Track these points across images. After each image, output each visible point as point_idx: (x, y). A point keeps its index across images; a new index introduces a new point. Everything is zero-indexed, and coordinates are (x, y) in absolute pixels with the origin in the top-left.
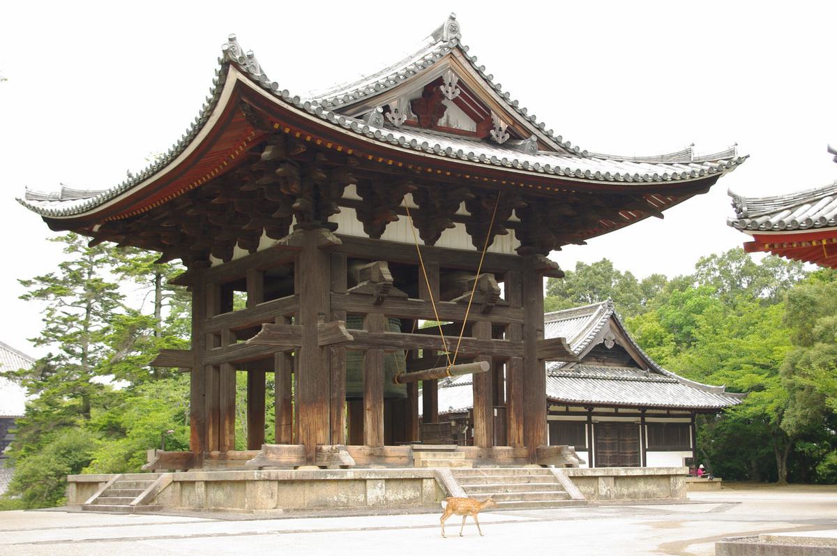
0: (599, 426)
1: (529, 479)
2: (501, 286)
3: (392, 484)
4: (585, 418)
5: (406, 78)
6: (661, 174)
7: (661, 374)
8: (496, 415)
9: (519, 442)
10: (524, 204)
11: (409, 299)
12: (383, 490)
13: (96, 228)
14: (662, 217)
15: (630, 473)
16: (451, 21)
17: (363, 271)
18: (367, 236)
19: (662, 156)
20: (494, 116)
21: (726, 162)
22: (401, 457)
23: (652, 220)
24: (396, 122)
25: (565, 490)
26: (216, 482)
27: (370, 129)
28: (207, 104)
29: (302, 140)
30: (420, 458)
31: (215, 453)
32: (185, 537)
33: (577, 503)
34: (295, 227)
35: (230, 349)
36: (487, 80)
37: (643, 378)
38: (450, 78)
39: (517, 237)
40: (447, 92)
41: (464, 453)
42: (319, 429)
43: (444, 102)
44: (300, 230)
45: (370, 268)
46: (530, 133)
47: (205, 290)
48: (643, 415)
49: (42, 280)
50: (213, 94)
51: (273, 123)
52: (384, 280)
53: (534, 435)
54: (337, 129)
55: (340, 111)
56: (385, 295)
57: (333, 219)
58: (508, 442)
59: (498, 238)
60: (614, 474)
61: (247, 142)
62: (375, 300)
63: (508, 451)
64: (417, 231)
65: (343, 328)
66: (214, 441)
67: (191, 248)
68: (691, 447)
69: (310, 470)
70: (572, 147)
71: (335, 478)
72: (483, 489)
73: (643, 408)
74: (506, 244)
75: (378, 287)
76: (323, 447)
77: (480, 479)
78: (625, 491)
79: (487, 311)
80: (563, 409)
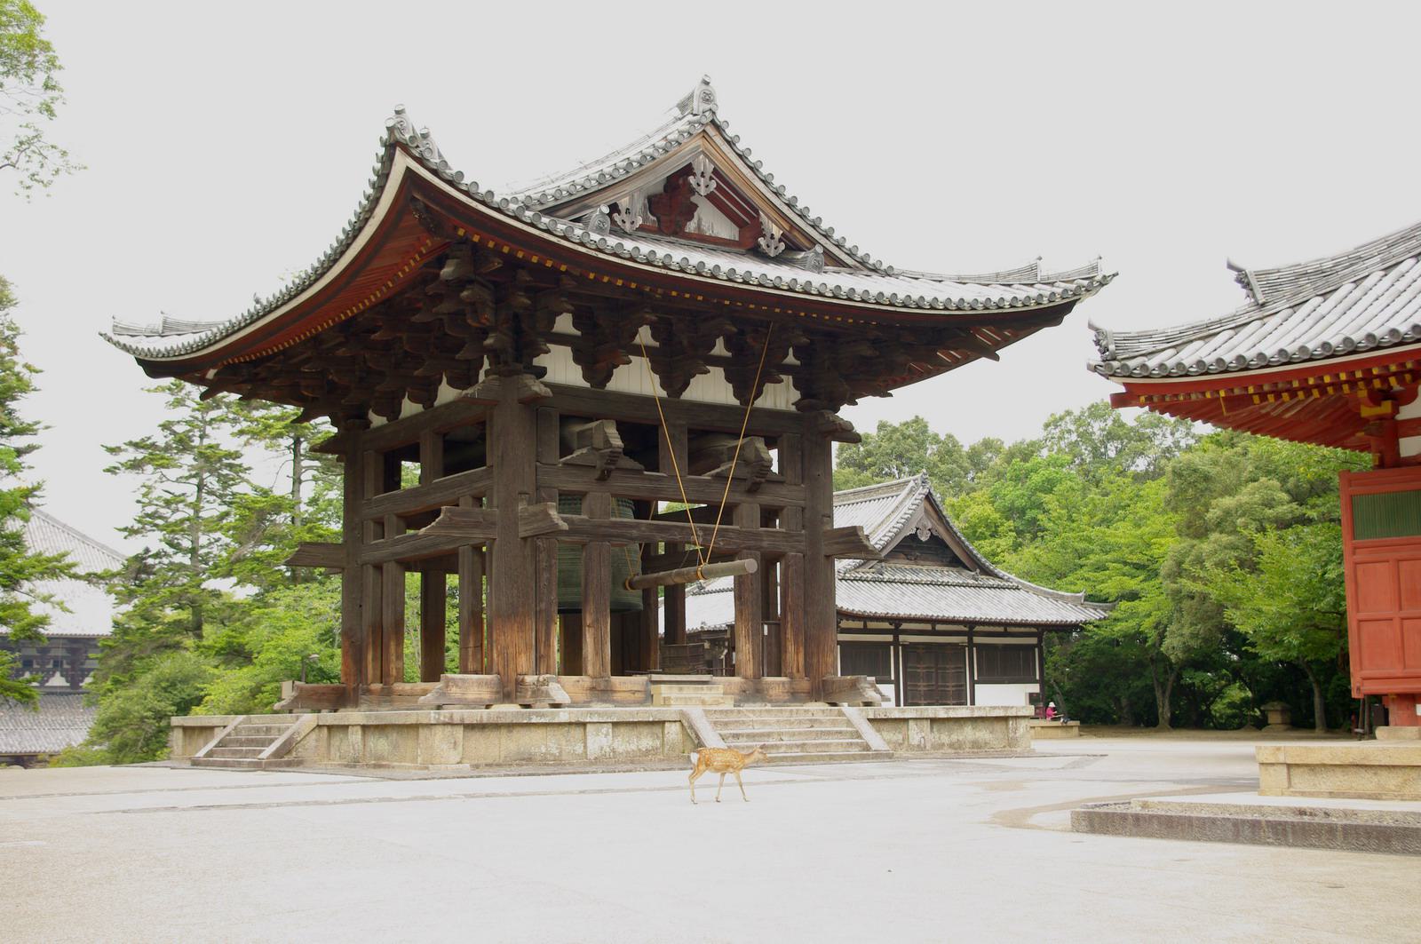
0: (910, 649)
1: (813, 722)
2: (774, 454)
3: (622, 730)
4: (890, 638)
5: (641, 165)
6: (995, 299)
7: (996, 576)
8: (766, 633)
9: (798, 671)
10: (804, 340)
11: (646, 473)
12: (610, 737)
13: (211, 374)
14: (997, 358)
15: (952, 714)
16: (704, 87)
17: (581, 434)
18: (587, 385)
19: (997, 275)
20: (763, 218)
21: (1086, 283)
22: (634, 692)
23: (983, 363)
24: (627, 227)
25: (862, 739)
26: (377, 727)
27: (589, 236)
28: (365, 202)
29: (497, 252)
30: (661, 694)
31: (377, 686)
32: (335, 803)
33: (878, 756)
34: (487, 373)
35: (397, 542)
36: (753, 169)
37: (971, 582)
38: (703, 165)
39: (796, 386)
40: (699, 185)
41: (721, 686)
42: (520, 654)
43: (694, 199)
44: (495, 376)
45: (591, 429)
46: (814, 242)
47: (363, 460)
48: (970, 634)
49: (136, 445)
50: (374, 188)
51: (456, 228)
52: (611, 446)
53: (819, 662)
54: (546, 236)
55: (550, 212)
56: (613, 467)
57: (539, 361)
58: (783, 670)
59: (769, 387)
60: (931, 716)
61: (421, 254)
62: (597, 474)
63: (783, 683)
64: (657, 378)
65: (554, 513)
66: (374, 669)
67: (343, 401)
68: (1038, 678)
69: (509, 710)
70: (871, 262)
71: (543, 720)
72: (748, 736)
73: (897, 621)
74: (780, 396)
75: (602, 456)
76: (526, 677)
77: (744, 722)
78: (945, 738)
79: (753, 490)
80: (860, 625)
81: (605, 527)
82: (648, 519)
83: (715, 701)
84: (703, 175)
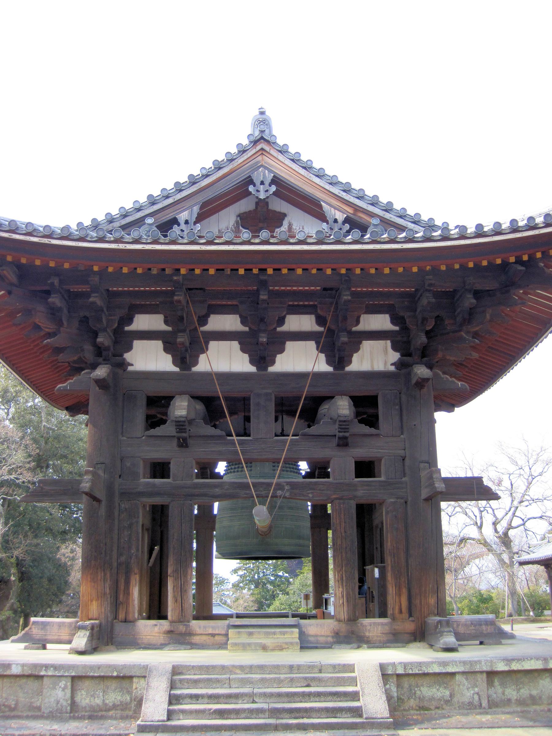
9: (401, 612)
18: (177, 369)
22: (213, 635)
39: (395, 348)
40: (258, 191)
42: (92, 601)
53: (421, 602)
56: (184, 435)
63: (382, 624)
64: (246, 357)
77: (218, 681)
81: (186, 488)
83: (277, 646)
84: (262, 183)
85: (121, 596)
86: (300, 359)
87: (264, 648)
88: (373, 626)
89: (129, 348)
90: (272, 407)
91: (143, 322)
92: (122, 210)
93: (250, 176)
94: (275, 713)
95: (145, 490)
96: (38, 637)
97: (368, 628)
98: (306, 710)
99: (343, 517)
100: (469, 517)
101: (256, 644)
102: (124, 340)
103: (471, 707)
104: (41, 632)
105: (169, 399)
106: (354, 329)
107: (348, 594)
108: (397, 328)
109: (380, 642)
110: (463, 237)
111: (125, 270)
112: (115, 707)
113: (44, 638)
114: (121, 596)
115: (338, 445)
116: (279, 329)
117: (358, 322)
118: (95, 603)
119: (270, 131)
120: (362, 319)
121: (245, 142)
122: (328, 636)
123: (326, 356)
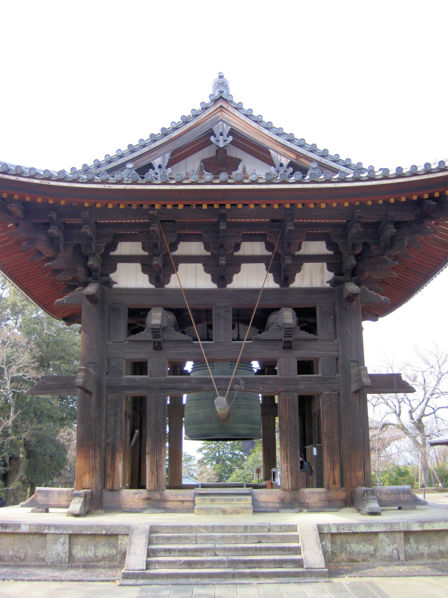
9: (334, 483)
18: (153, 287)
22: (183, 501)
40: (218, 141)
42: (85, 474)
53: (351, 474)
54: (6, 177)
56: (159, 340)
63: (320, 493)
64: (209, 276)
77: (187, 538)
82: (264, 375)
84: (221, 134)
85: (109, 471)
86: (253, 278)
87: (224, 512)
88: (312, 494)
89: (114, 269)
90: (230, 317)
91: (125, 248)
92: (108, 157)
93: (211, 129)
94: (233, 564)
95: (127, 384)
96: (42, 503)
97: (308, 496)
98: (258, 562)
99: (288, 406)
100: (390, 407)
101: (218, 509)
102: (110, 263)
103: (391, 560)
104: (46, 499)
105: (147, 310)
106: (297, 253)
107: (292, 469)
108: (331, 253)
109: (318, 507)
110: (386, 178)
111: (110, 206)
112: (104, 558)
113: (47, 503)
114: (109, 470)
115: (284, 348)
116: (235, 254)
117: (300, 248)
118: (87, 475)
119: (228, 91)
120: (303, 245)
121: (207, 101)
122: (275, 503)
123: (274, 276)
